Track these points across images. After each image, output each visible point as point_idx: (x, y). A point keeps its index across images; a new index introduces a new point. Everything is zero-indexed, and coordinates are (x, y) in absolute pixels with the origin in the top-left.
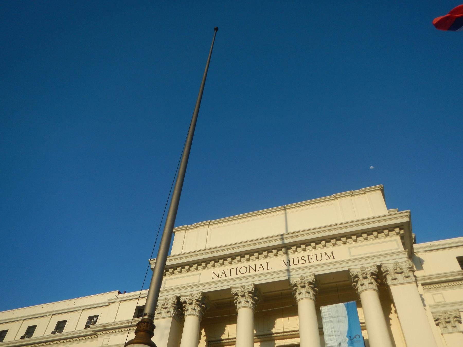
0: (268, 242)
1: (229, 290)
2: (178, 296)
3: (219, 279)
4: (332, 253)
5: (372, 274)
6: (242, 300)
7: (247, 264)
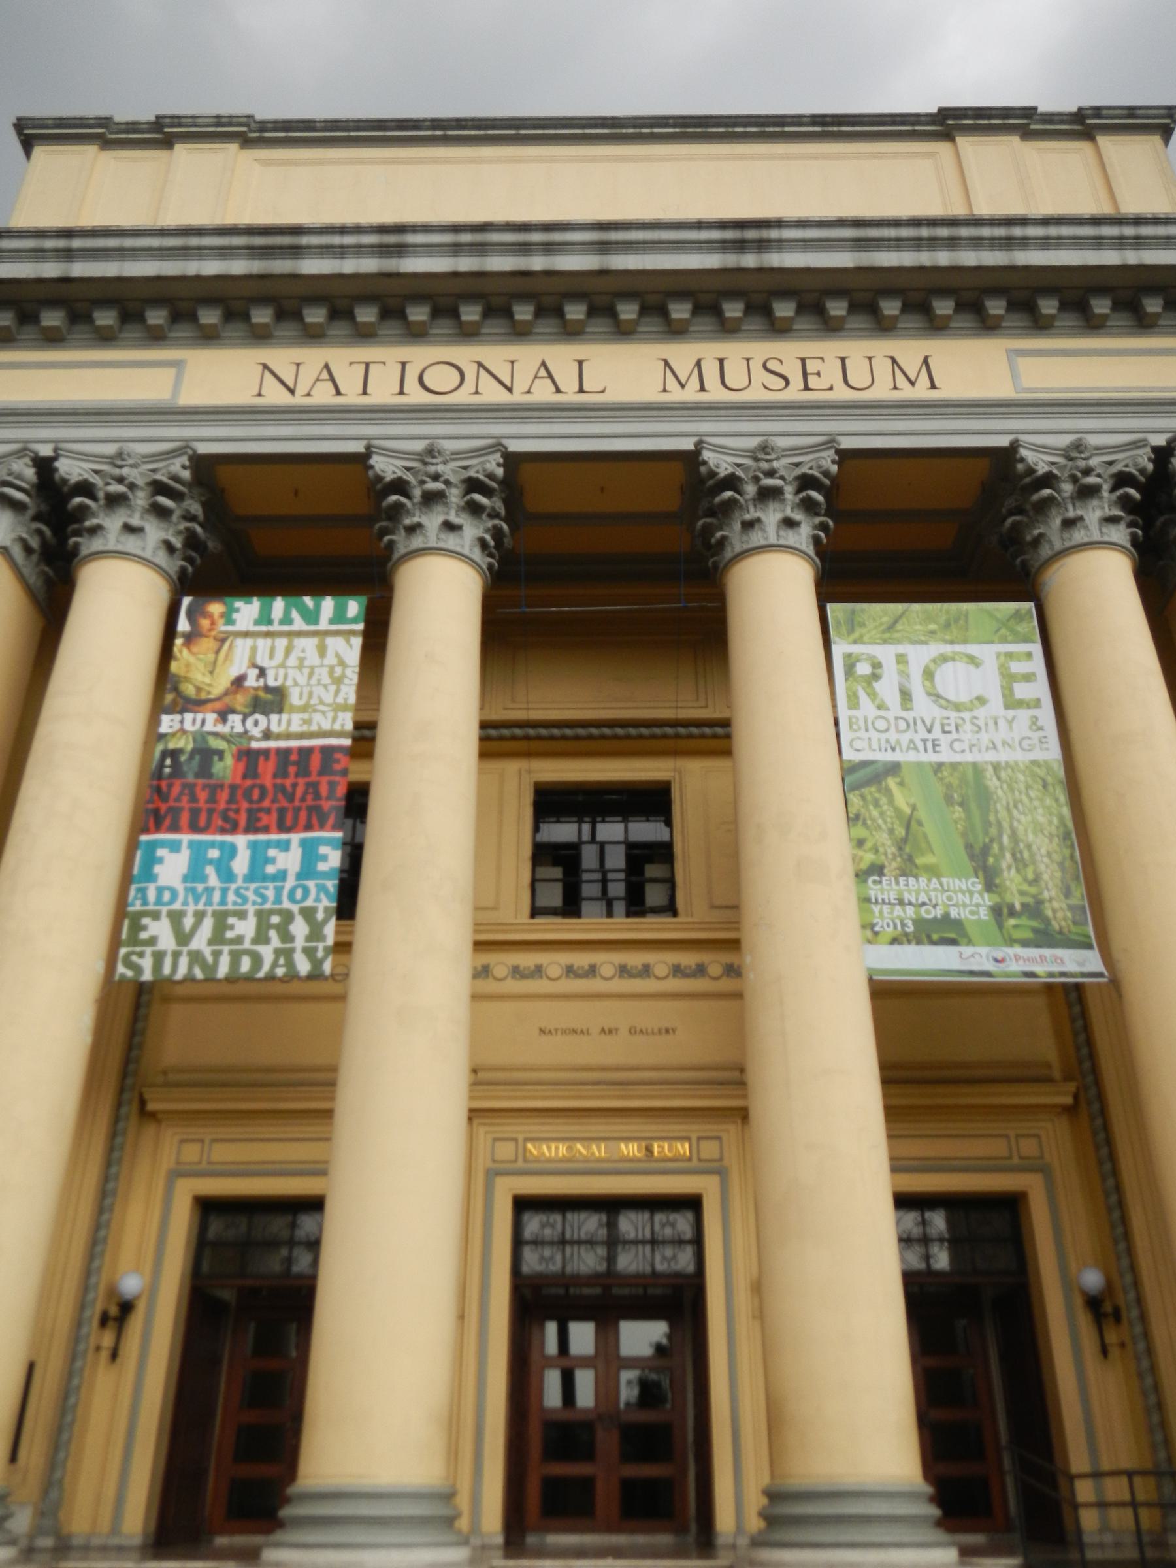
0: (604, 247)
1: (361, 460)
2: (46, 451)
3: (299, 400)
4: (926, 361)
5: (1122, 480)
6: (424, 520)
7: (465, 354)
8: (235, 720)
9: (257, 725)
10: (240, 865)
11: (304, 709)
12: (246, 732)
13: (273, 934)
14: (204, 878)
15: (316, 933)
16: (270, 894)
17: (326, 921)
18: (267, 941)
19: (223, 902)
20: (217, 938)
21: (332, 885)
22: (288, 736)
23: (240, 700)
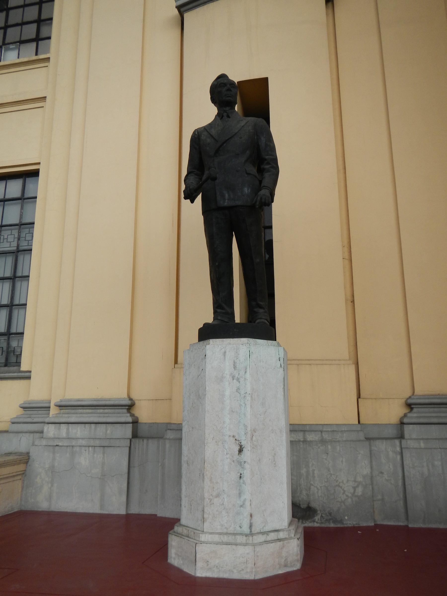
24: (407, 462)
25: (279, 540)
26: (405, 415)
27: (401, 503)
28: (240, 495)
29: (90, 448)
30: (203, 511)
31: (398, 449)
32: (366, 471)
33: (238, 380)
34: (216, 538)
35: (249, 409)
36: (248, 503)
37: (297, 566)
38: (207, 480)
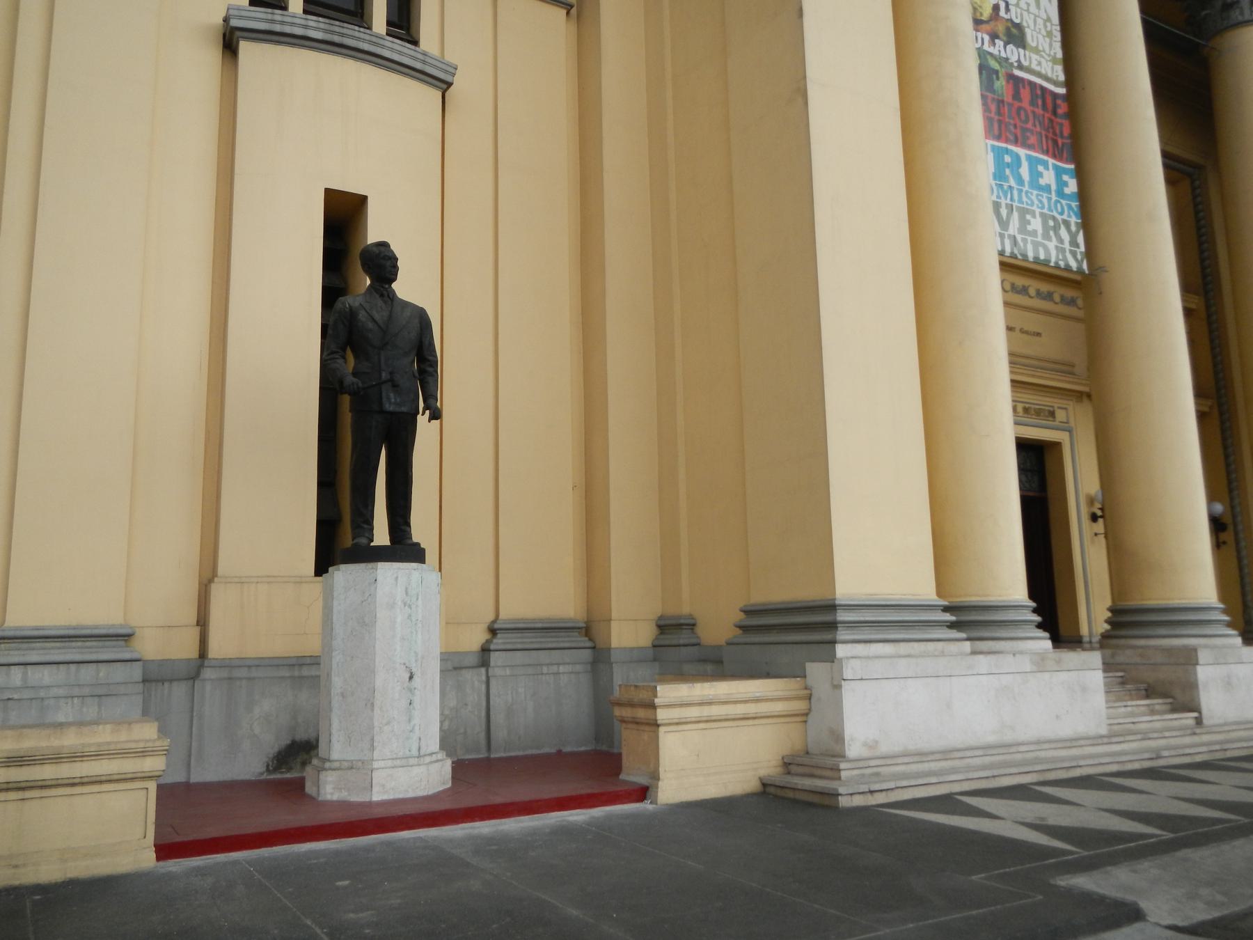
8: (999, 43)
9: (1013, 53)
10: (1025, 171)
11: (1036, 50)
12: (1007, 59)
13: (1052, 233)
14: (1006, 179)
15: (1074, 243)
16: (1045, 201)
17: (1078, 232)
18: (1049, 239)
19: (1020, 201)
20: (1023, 229)
21: (1075, 204)
22: (1029, 70)
23: (1001, 28)
24: (493, 691)
25: (437, 761)
26: (488, 642)
27: (483, 735)
28: (410, 721)
29: (76, 700)
30: (373, 739)
31: (484, 678)
32: (453, 703)
33: (410, 607)
34: (390, 763)
35: (420, 636)
36: (417, 728)
37: (449, 785)
38: (377, 711)
